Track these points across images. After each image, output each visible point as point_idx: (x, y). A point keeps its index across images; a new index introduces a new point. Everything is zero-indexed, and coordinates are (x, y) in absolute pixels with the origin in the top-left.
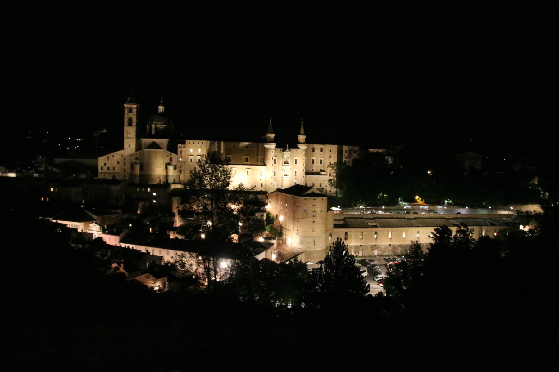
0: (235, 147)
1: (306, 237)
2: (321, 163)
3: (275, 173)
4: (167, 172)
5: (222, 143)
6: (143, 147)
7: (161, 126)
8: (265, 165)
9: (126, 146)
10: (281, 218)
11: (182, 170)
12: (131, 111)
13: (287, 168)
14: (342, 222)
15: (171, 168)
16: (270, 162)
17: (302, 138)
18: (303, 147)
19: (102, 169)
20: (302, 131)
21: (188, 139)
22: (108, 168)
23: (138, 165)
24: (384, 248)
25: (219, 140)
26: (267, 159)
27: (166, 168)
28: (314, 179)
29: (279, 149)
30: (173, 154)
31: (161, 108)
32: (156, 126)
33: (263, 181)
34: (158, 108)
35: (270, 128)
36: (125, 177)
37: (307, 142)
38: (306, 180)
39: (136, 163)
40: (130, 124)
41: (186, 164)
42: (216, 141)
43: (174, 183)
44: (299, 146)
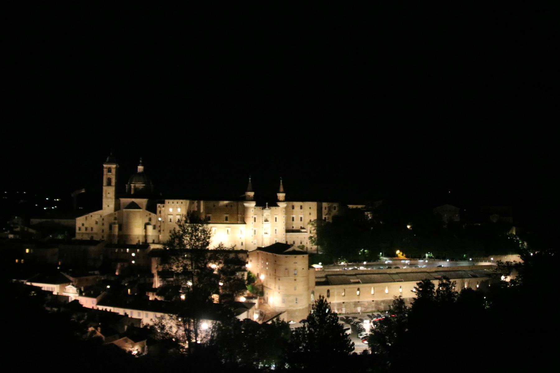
0: (214, 206)
1: (289, 296)
2: (301, 220)
3: (255, 231)
4: (146, 232)
5: (202, 202)
6: (122, 206)
7: (140, 185)
8: (245, 223)
9: (105, 205)
10: (262, 277)
11: (162, 229)
12: (110, 171)
13: (267, 226)
14: (323, 280)
15: (150, 228)
17: (281, 196)
18: (282, 205)
19: (80, 229)
20: (282, 189)
22: (86, 229)
23: (117, 226)
24: (367, 304)
25: (199, 199)
26: (247, 217)
27: (145, 228)
29: (258, 208)
31: (140, 168)
32: (135, 186)
33: (243, 240)
34: (137, 168)
35: (250, 186)
36: (103, 237)
37: (287, 200)
38: (286, 238)
39: (114, 223)
40: (109, 184)
42: (195, 200)
43: (153, 243)
44: (279, 204)
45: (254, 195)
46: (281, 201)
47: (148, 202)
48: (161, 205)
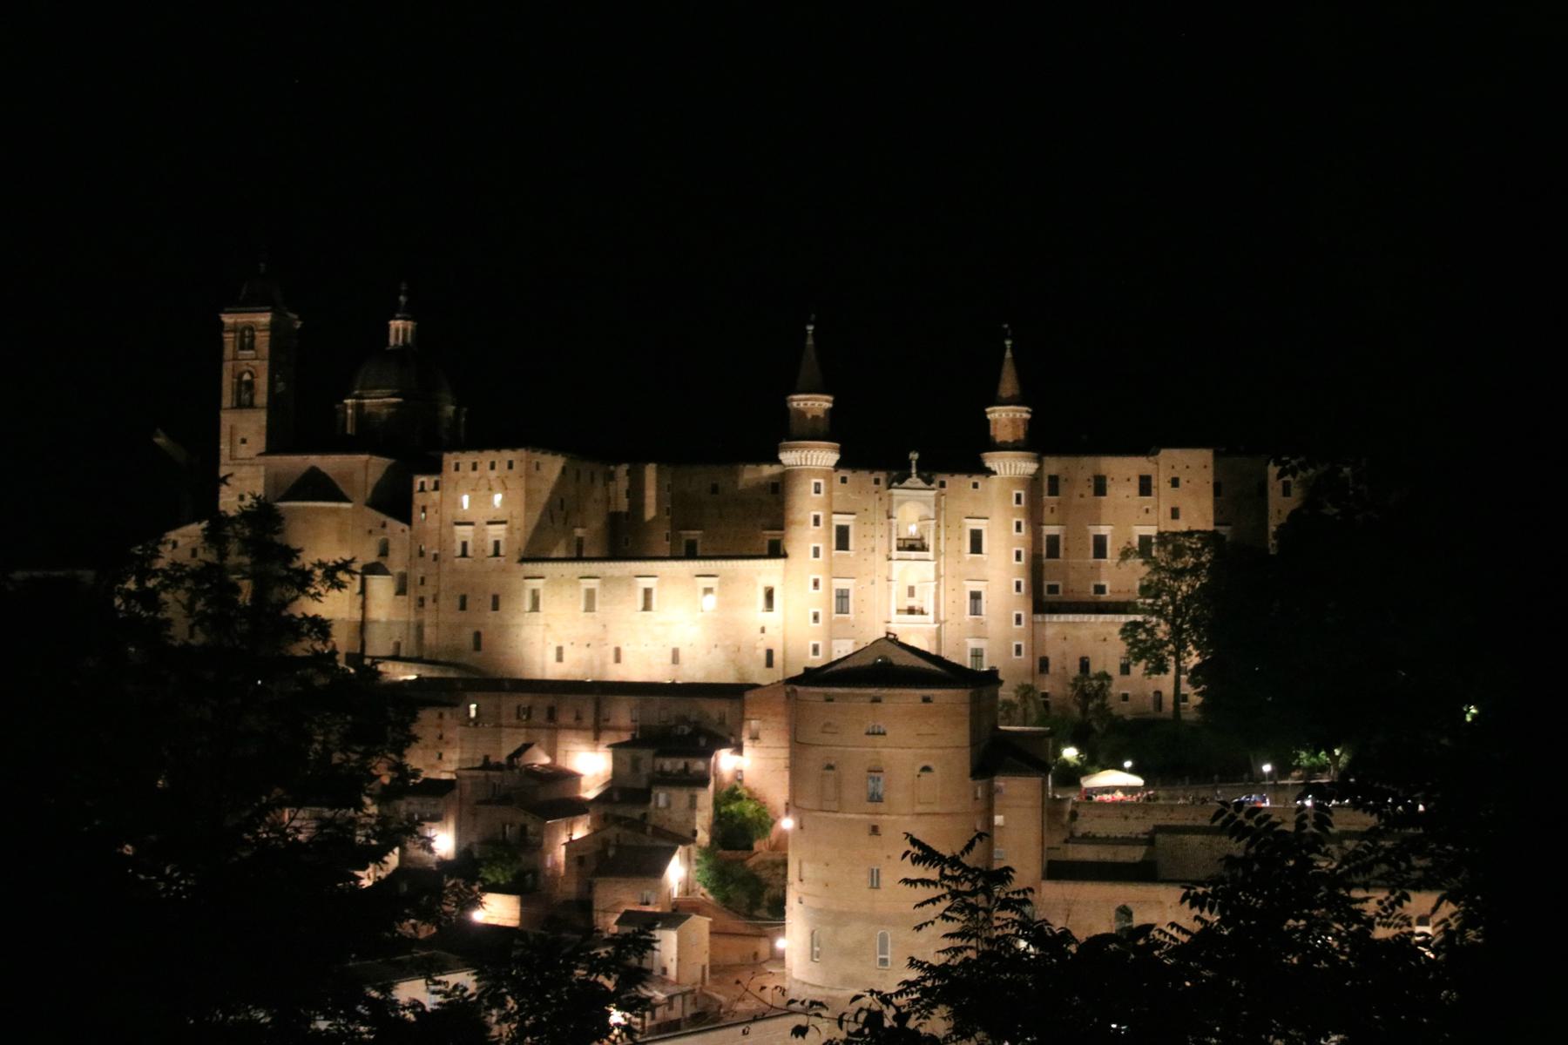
3: (843, 596)
4: (364, 607)
5: (651, 472)
7: (379, 402)
8: (785, 556)
10: (787, 823)
12: (249, 339)
13: (916, 572)
14: (1136, 854)
15: (381, 587)
16: (806, 537)
17: (1005, 418)
18: (1010, 467)
20: (1008, 385)
21: (451, 449)
25: (637, 460)
26: (792, 523)
28: (1084, 633)
29: (865, 478)
30: (389, 521)
32: (359, 408)
33: (774, 639)
34: (388, 327)
35: (810, 365)
37: (1035, 441)
38: (1035, 637)
41: (446, 567)
42: (618, 462)
43: (396, 658)
44: (994, 460)
45: (830, 412)
47: (390, 469)
48: (428, 481)
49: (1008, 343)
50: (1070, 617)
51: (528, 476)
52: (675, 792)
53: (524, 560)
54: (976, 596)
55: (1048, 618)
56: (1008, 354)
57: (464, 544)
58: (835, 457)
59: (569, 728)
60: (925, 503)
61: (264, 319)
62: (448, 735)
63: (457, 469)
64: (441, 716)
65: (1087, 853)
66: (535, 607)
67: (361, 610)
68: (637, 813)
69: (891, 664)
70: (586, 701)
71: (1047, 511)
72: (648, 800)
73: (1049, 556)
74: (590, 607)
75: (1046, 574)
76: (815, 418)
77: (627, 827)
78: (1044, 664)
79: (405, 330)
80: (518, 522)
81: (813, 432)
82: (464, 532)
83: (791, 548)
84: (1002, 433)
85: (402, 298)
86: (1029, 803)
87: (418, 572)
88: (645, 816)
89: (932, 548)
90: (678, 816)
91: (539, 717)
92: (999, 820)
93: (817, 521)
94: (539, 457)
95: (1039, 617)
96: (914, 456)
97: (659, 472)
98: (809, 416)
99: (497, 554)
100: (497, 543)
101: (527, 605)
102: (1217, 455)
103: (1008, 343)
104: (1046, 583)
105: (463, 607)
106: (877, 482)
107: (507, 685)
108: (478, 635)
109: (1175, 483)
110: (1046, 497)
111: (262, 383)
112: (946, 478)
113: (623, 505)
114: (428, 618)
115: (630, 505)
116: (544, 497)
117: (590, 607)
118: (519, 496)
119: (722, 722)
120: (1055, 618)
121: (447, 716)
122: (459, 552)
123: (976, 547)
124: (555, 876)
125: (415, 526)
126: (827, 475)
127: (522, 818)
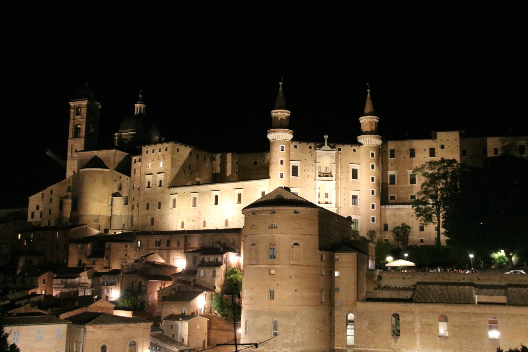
0: (255, 163)
4: (111, 211)
5: (229, 156)
8: (269, 178)
15: (118, 202)
17: (367, 121)
18: (369, 142)
20: (368, 108)
23: (70, 201)
25: (223, 151)
28: (403, 213)
29: (304, 146)
32: (120, 136)
39: (66, 197)
40: (76, 135)
44: (361, 139)
46: (367, 133)
49: (369, 91)
50: (397, 207)
51: (173, 153)
52: (207, 269)
53: (170, 187)
54: (355, 197)
55: (387, 207)
56: (369, 95)
57: (149, 183)
58: (291, 136)
59: (175, 249)
60: (331, 156)
61: (85, 103)
62: (129, 254)
63: (147, 153)
64: (126, 246)
65: (386, 294)
66: (174, 207)
67: (103, 206)
68: (191, 279)
69: (283, 199)
70: (182, 239)
71: (390, 164)
72: (197, 274)
73: (390, 184)
74: (195, 205)
75: (389, 191)
76: (282, 119)
77: (182, 283)
78: (386, 227)
79: (140, 108)
80: (168, 172)
81: (281, 125)
82: (149, 178)
83: (271, 174)
84: (365, 128)
85: (140, 96)
86: (351, 265)
87: (133, 195)
88: (194, 281)
89: (334, 176)
90: (208, 281)
91: (163, 245)
92: (337, 274)
93: (282, 162)
94: (178, 146)
95: (384, 207)
96: (326, 137)
97: (233, 157)
98: (279, 119)
99: (160, 186)
100: (161, 181)
101: (171, 205)
102: (461, 136)
103: (369, 91)
104: (390, 195)
105: (148, 208)
106: (310, 148)
107: (153, 233)
108: (153, 219)
109: (442, 147)
110: (389, 159)
111: (83, 128)
112: (341, 146)
113: (218, 170)
114: (135, 214)
115: (221, 170)
116: (181, 163)
117: (195, 205)
118: (169, 161)
119: (234, 243)
120: (390, 207)
121: (129, 246)
122: (147, 186)
123: (355, 174)
124: (153, 306)
125: (132, 177)
126: (287, 143)
127: (140, 280)
